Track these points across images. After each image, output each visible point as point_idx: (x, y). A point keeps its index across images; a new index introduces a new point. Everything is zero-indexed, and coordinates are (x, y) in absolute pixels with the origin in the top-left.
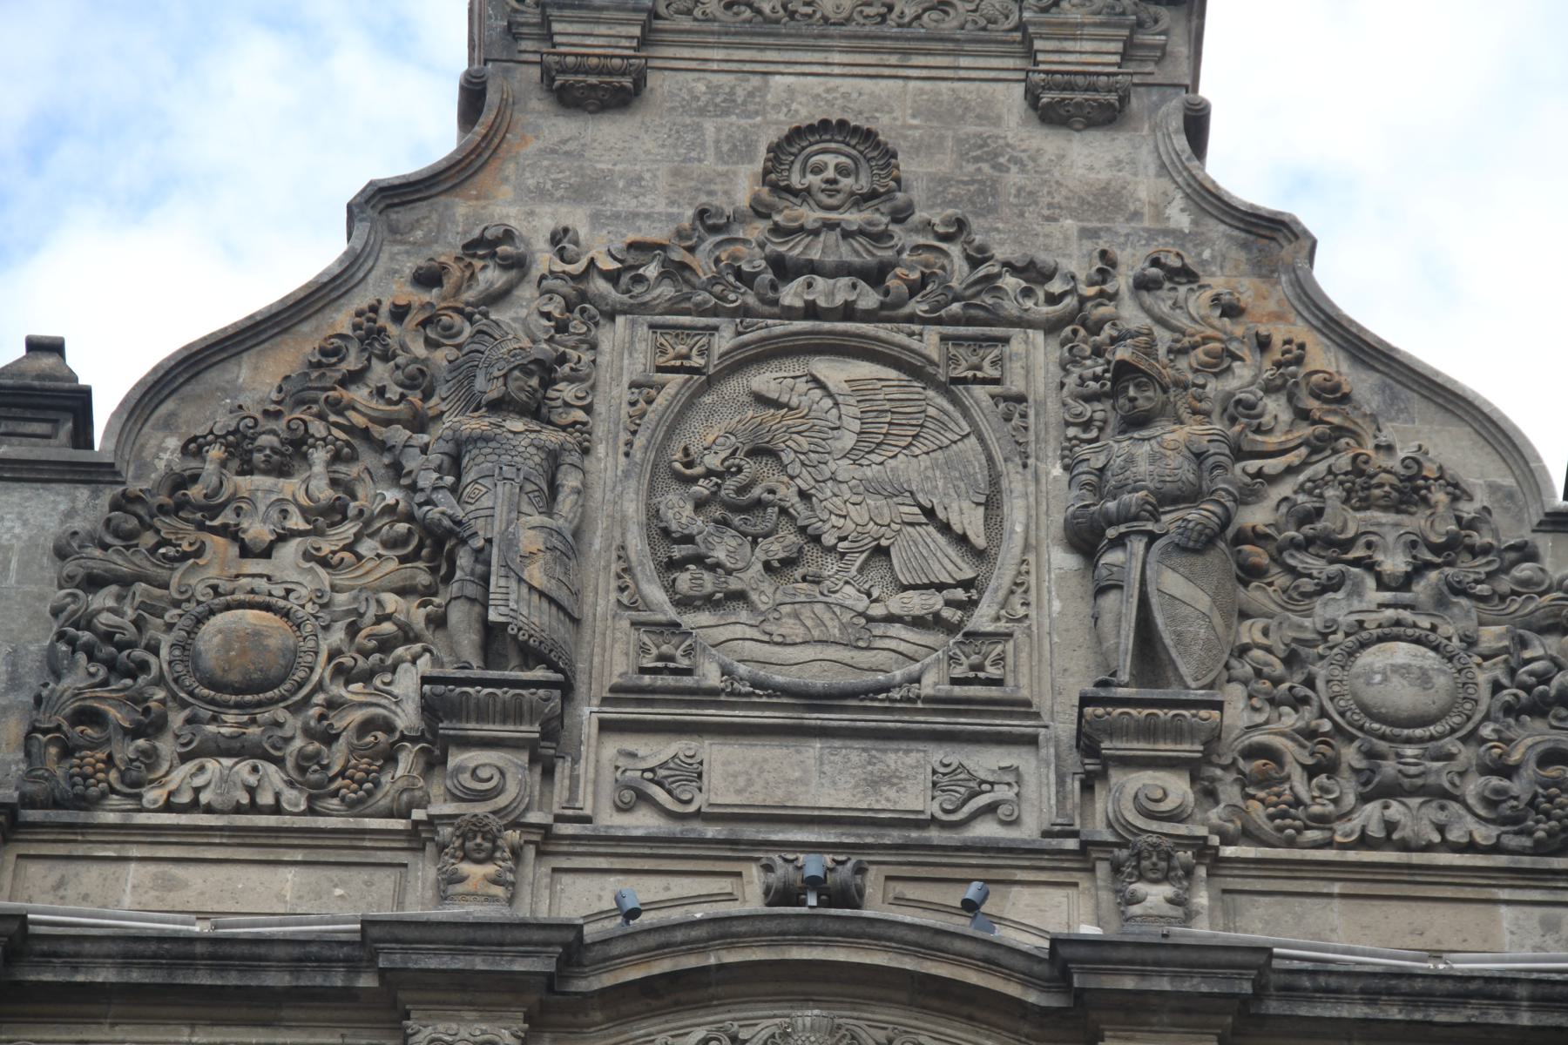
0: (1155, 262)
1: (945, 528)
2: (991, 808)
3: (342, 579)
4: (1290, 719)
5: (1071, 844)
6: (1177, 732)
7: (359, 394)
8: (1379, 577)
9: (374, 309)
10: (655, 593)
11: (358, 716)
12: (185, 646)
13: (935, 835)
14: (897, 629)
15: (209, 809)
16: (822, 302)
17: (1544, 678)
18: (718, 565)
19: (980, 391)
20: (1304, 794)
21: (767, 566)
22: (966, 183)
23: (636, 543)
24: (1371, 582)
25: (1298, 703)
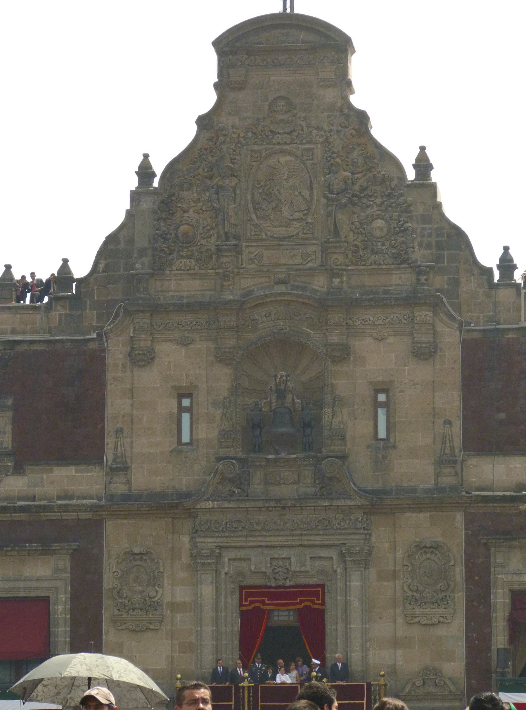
0: (340, 125)
1: (302, 196)
2: (311, 260)
3: (201, 216)
4: (361, 238)
5: (323, 268)
6: (341, 247)
7: (200, 170)
8: (376, 205)
9: (201, 149)
10: (254, 217)
11: (206, 248)
12: (176, 234)
13: (301, 267)
14: (295, 222)
15: (183, 270)
16: (280, 142)
17: (402, 225)
18: (264, 209)
19: (308, 162)
20: (361, 254)
21: (272, 208)
22: (307, 104)
23: (250, 206)
24: (375, 206)
25: (361, 233)
